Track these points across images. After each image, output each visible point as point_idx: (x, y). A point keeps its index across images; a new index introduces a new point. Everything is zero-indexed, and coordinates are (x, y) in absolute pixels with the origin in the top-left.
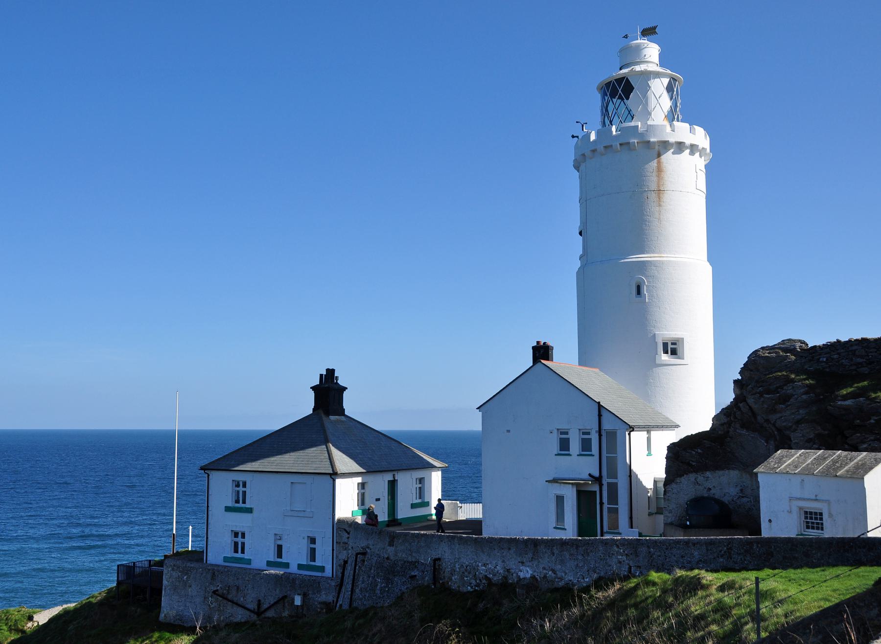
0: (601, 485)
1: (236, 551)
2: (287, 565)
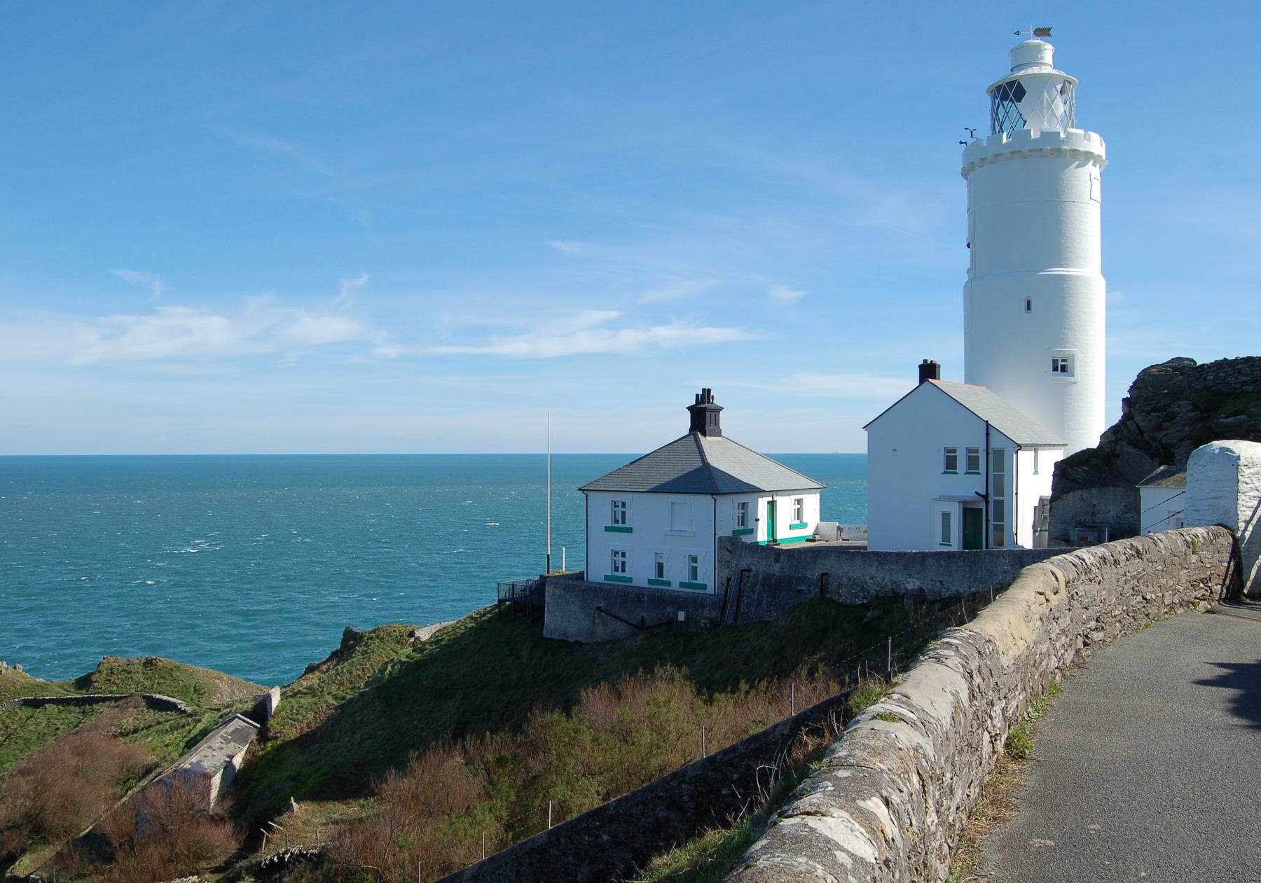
0: (987, 503)
1: (616, 569)
2: (668, 583)
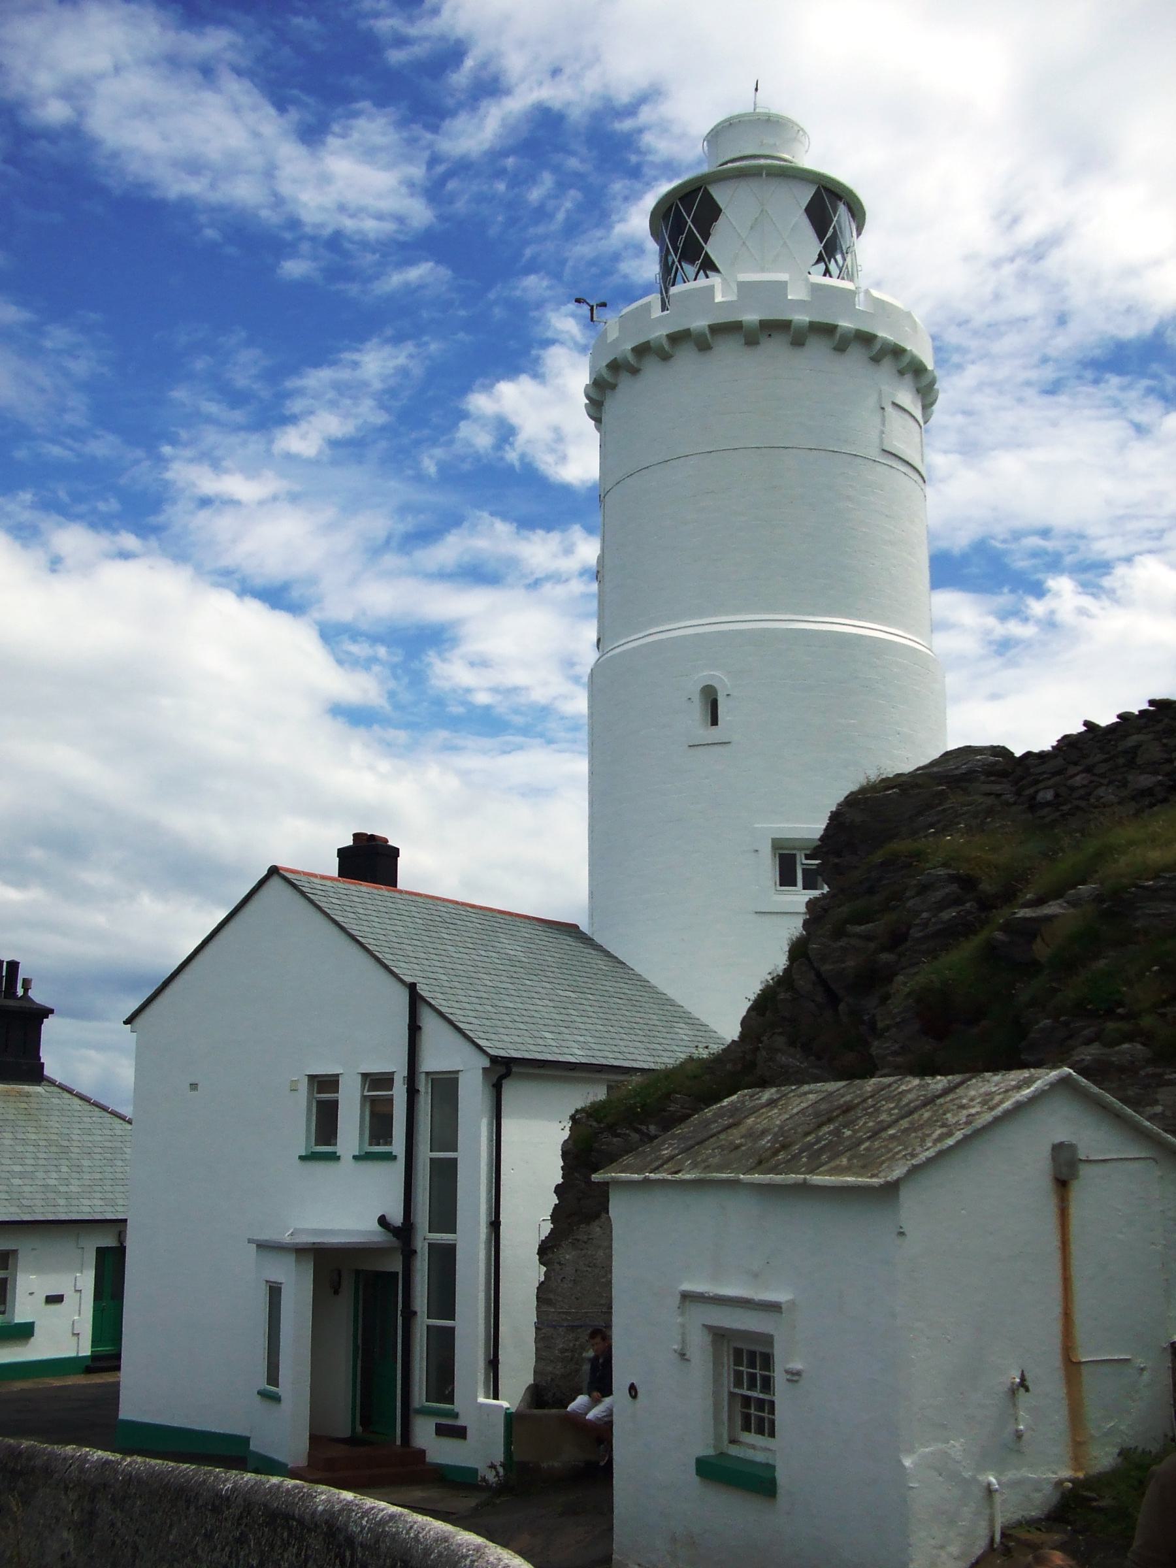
0: (409, 1254)
